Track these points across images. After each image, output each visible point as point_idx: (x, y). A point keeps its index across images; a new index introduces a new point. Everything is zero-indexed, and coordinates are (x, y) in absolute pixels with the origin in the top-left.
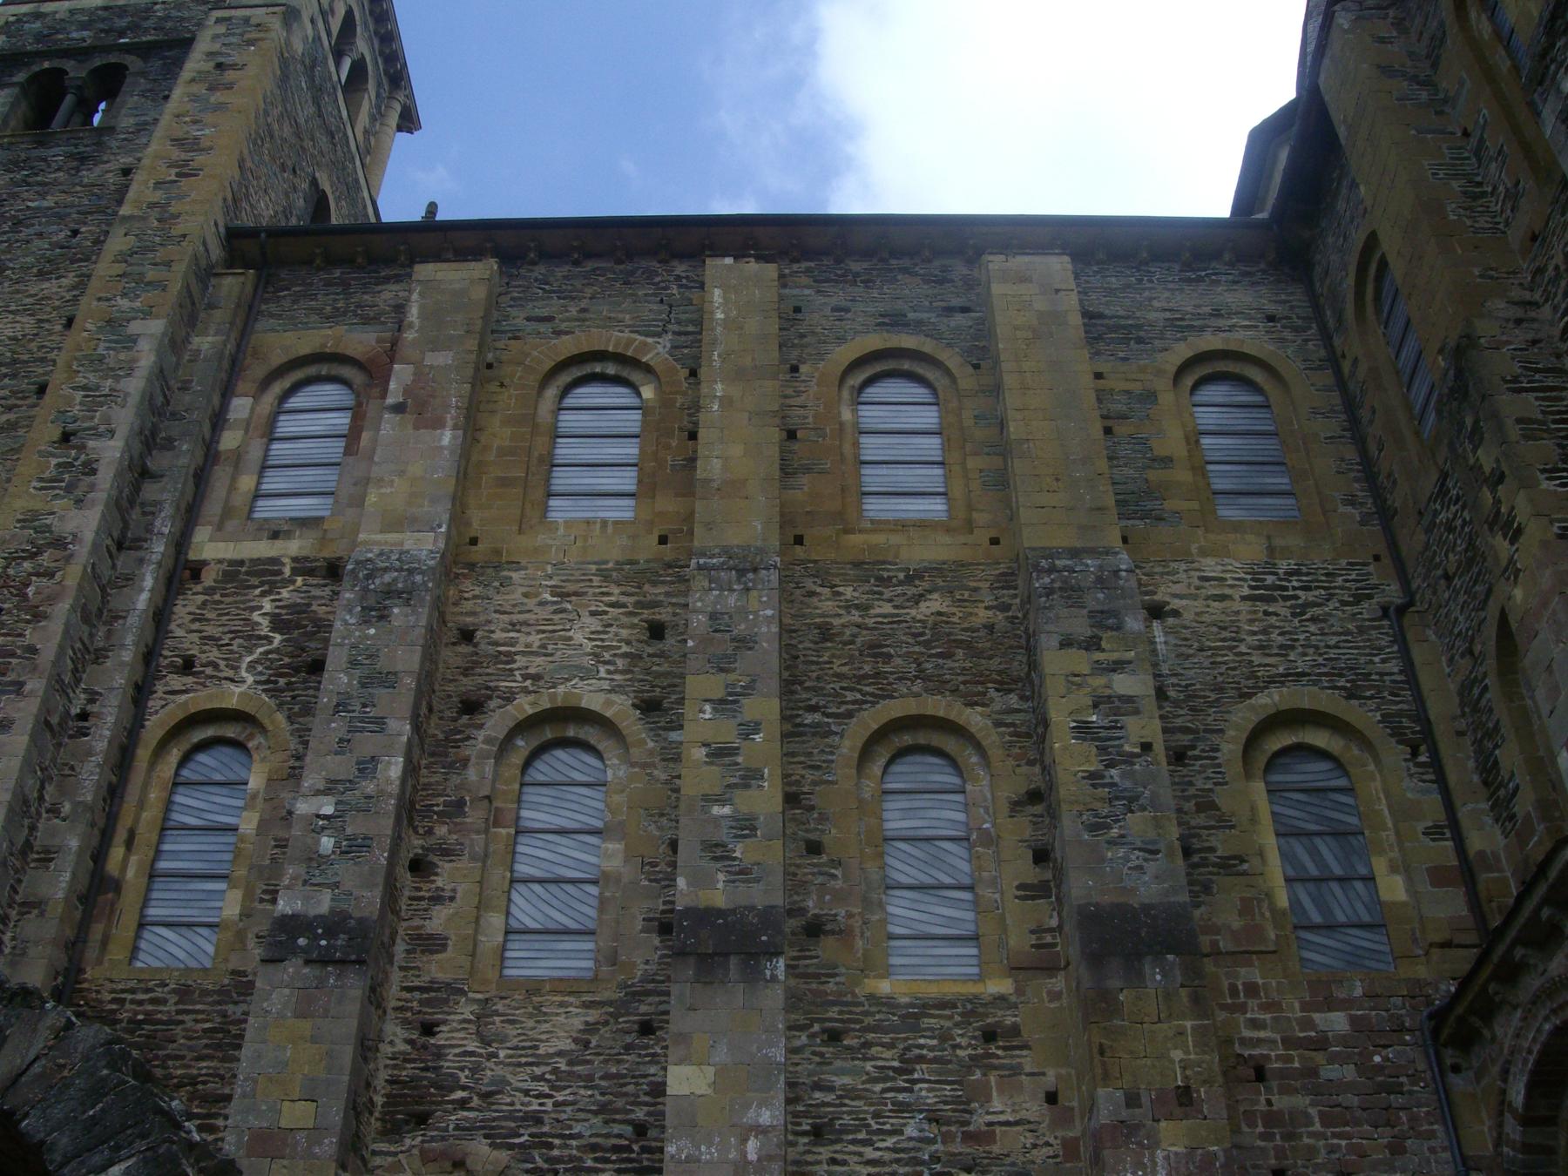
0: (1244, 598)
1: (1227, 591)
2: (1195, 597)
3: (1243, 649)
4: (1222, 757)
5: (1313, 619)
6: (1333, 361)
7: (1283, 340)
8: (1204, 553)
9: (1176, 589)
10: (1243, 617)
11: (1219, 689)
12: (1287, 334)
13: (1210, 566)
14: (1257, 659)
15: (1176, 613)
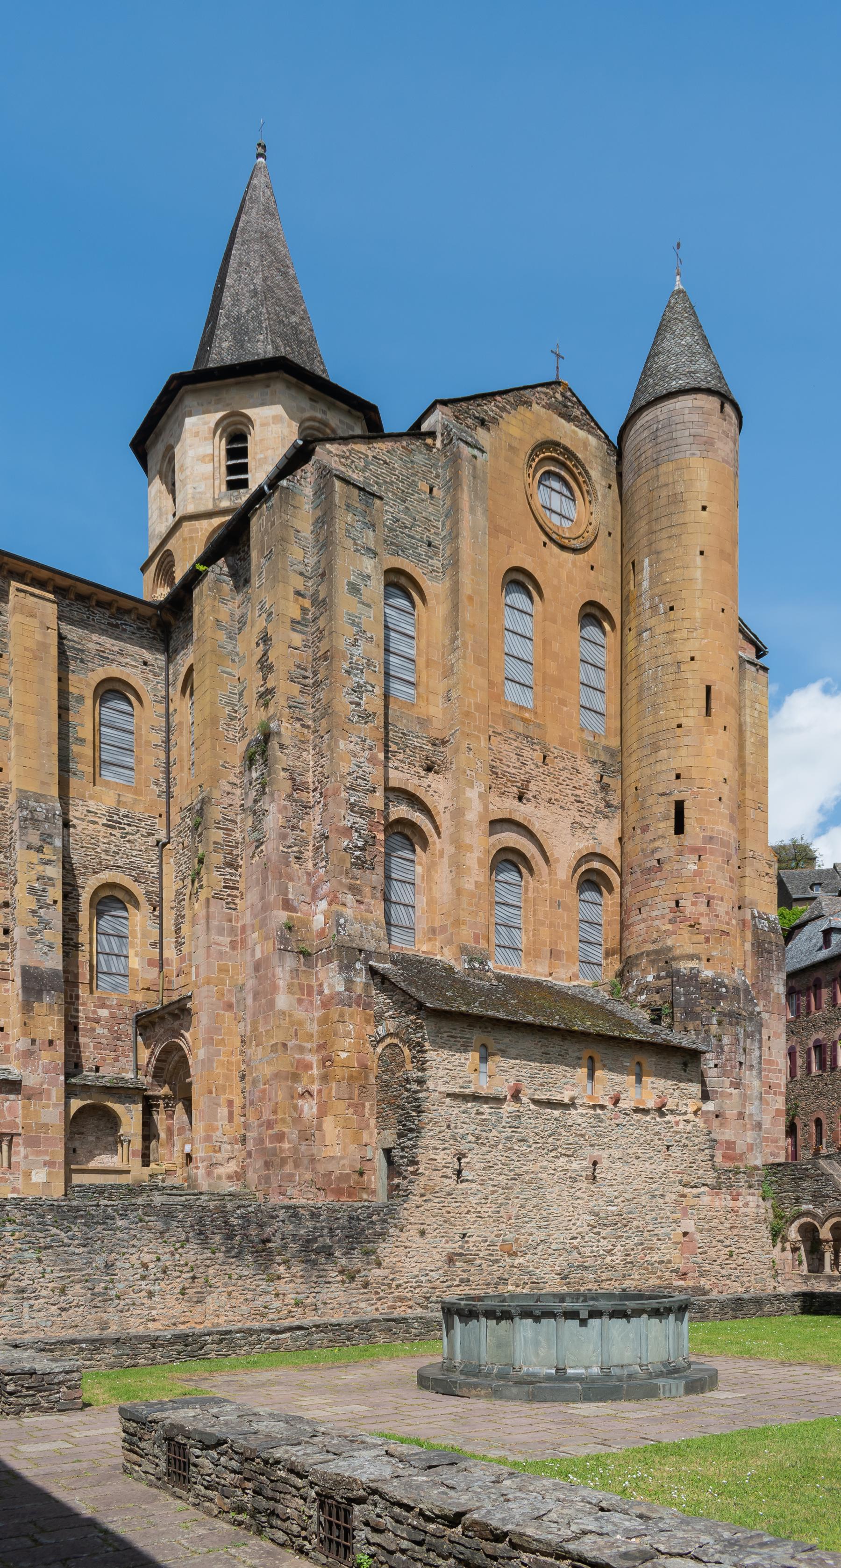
0: (103, 825)
1: (97, 820)
2: (83, 820)
3: (98, 850)
4: (82, 899)
5: (129, 841)
6: (167, 699)
7: (148, 679)
8: (91, 797)
9: (77, 814)
10: (102, 834)
11: (85, 867)
12: (151, 676)
13: (92, 805)
14: (103, 856)
15: (74, 826)
